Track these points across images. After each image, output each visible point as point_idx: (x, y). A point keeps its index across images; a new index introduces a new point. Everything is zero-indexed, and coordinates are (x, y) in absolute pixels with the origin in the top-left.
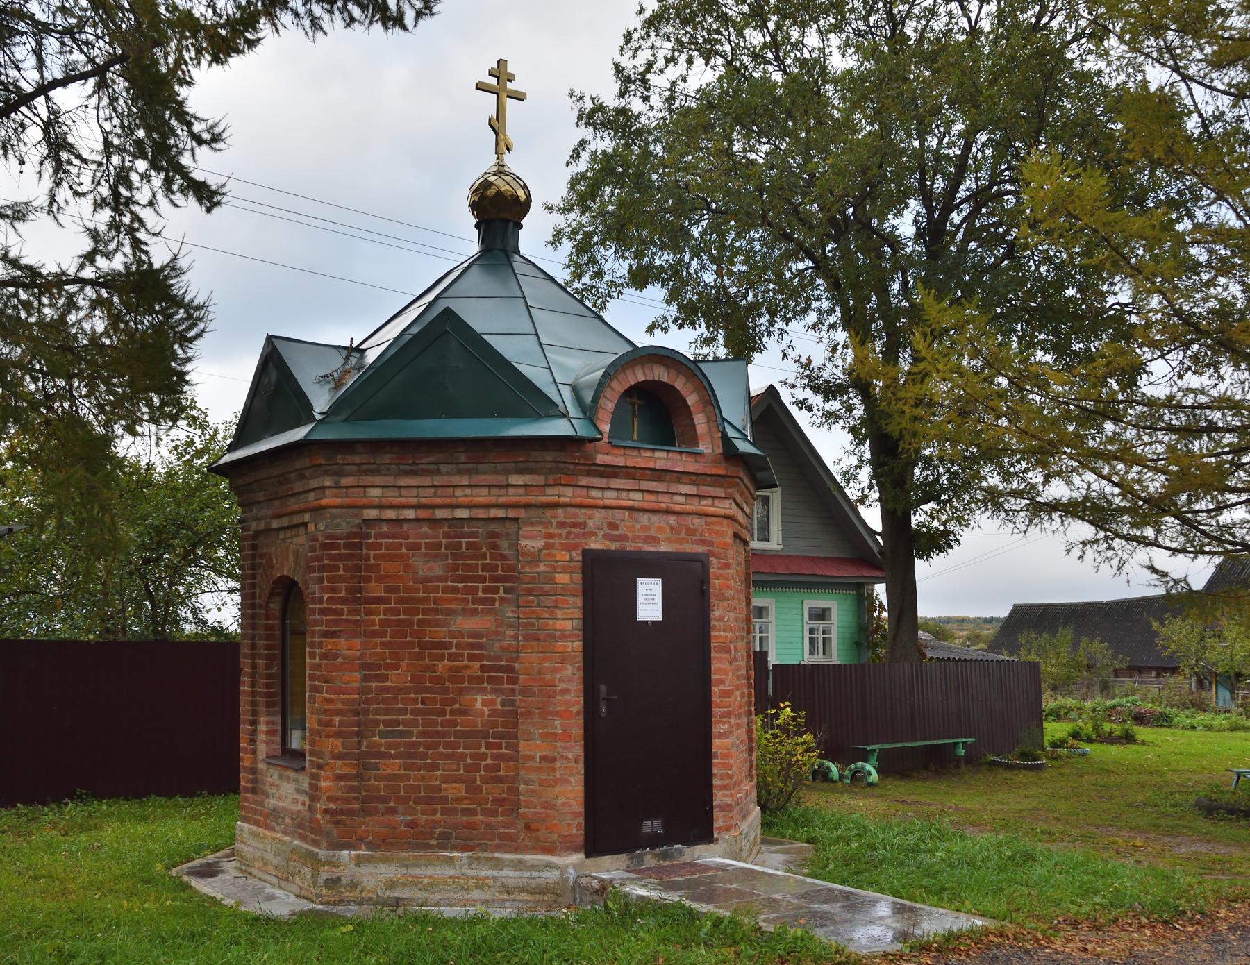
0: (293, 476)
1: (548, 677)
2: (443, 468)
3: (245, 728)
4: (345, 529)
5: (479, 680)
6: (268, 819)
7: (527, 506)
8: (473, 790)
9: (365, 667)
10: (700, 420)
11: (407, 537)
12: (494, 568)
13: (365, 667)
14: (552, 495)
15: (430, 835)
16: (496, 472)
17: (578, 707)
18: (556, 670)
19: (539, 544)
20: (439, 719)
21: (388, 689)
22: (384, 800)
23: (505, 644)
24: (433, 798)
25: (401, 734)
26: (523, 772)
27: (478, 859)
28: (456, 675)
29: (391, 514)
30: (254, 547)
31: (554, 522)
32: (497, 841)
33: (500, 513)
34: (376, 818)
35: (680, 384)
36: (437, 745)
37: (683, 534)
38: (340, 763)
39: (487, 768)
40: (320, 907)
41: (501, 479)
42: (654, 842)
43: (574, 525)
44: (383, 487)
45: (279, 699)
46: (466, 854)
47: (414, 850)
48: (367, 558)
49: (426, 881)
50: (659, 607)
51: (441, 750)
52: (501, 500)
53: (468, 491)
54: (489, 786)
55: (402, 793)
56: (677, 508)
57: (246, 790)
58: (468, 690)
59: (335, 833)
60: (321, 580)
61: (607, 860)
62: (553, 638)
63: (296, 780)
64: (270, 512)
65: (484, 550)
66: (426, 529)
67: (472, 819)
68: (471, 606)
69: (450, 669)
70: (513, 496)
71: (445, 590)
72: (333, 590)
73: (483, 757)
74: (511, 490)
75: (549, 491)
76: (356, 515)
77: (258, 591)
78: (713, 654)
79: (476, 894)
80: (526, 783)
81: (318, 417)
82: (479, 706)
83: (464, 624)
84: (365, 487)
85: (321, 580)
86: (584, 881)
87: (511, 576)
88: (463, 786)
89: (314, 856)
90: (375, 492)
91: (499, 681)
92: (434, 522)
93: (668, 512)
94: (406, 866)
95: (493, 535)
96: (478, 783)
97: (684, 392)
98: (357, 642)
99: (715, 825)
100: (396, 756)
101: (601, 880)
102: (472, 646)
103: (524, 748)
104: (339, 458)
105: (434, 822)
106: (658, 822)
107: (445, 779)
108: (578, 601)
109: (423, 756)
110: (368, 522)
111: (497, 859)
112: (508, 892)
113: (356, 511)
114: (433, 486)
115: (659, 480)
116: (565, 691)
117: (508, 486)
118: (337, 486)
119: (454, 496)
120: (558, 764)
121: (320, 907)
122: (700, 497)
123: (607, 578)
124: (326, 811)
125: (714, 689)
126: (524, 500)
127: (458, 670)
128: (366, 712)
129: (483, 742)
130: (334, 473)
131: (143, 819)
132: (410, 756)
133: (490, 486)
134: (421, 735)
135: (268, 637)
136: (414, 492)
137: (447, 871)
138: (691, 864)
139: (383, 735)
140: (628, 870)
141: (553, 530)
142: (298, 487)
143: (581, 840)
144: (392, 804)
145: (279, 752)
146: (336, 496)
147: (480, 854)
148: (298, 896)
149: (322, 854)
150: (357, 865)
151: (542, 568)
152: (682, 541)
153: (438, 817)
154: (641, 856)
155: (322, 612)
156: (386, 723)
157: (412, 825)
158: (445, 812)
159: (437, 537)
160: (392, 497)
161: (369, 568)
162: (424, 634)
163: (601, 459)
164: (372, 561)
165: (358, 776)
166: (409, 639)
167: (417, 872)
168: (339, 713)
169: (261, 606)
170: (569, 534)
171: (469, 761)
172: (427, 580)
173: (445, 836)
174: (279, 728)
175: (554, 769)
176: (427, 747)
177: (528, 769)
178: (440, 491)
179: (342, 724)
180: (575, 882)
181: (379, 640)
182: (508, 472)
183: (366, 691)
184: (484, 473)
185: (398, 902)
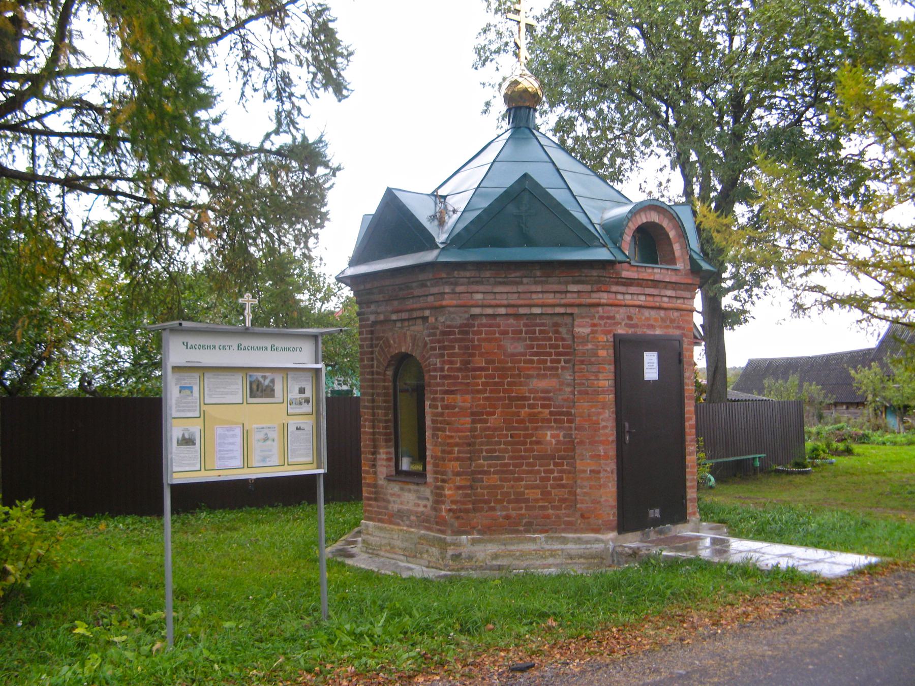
0: (414, 284)
1: (594, 418)
2: (525, 280)
3: (366, 458)
4: (458, 321)
5: (549, 421)
6: (395, 518)
7: (579, 305)
8: (546, 494)
9: (473, 414)
10: (677, 247)
11: (499, 327)
12: (557, 347)
13: (473, 414)
14: (595, 298)
15: (518, 524)
16: (559, 283)
17: (613, 438)
18: (599, 414)
19: (587, 330)
20: (523, 448)
21: (488, 428)
22: (487, 502)
23: (566, 396)
24: (519, 499)
25: (498, 458)
26: (579, 481)
27: (552, 538)
28: (533, 418)
29: (490, 311)
30: (372, 332)
31: (597, 316)
32: (563, 526)
33: (562, 310)
34: (482, 513)
35: (665, 224)
36: (522, 465)
37: (668, 323)
38: (458, 478)
39: (555, 479)
40: (449, 573)
41: (562, 288)
42: (655, 523)
43: (609, 318)
44: (484, 293)
45: (393, 437)
46: (543, 535)
47: (509, 533)
48: (473, 341)
49: (518, 553)
50: (656, 370)
51: (524, 467)
52: (563, 301)
53: (540, 296)
54: (556, 490)
55: (499, 497)
56: (665, 305)
57: (369, 499)
58: (541, 428)
59: (456, 524)
60: (442, 356)
61: (630, 536)
62: (597, 392)
63: (418, 491)
64: (389, 308)
65: (551, 334)
66: (511, 321)
67: (546, 513)
68: (542, 372)
69: (530, 414)
70: (570, 298)
71: (525, 362)
72: (451, 362)
73: (552, 472)
74: (569, 295)
75: (594, 295)
76: (465, 312)
77: (375, 363)
78: (686, 401)
79: (551, 561)
80: (581, 488)
81: (441, 246)
82: (548, 438)
83: (542, 384)
84: (472, 293)
85: (442, 356)
86: (619, 549)
87: (569, 352)
88: (539, 491)
89: (444, 541)
90: (479, 296)
91: (561, 421)
92: (517, 316)
93: (660, 308)
94: (505, 545)
95: (556, 325)
96: (549, 488)
97: (668, 229)
98: (468, 397)
99: (688, 512)
100: (495, 473)
101: (630, 548)
102: (544, 399)
103: (579, 466)
104: (456, 274)
105: (522, 515)
106: (657, 511)
107: (527, 487)
108: (612, 367)
109: (513, 472)
110: (474, 317)
111: (565, 538)
112: (571, 558)
113: (465, 309)
114: (519, 292)
115: (655, 287)
116: (605, 427)
117: (567, 292)
118: (454, 293)
119: (531, 299)
120: (602, 475)
121: (449, 573)
122: (677, 298)
123: (627, 351)
124: (450, 510)
125: (687, 424)
126: (578, 301)
127: (534, 415)
128: (474, 444)
129: (552, 462)
130: (452, 284)
131: (258, 521)
132: (503, 472)
133: (554, 292)
134: (511, 458)
135: (386, 395)
136: (505, 296)
137: (531, 547)
138: (676, 537)
139: (485, 459)
140: (641, 541)
141: (596, 321)
142: (417, 292)
143: (615, 523)
144: (492, 504)
145: (394, 473)
146: (452, 299)
147: (552, 535)
148: (427, 567)
149: (449, 538)
150: (472, 544)
151: (590, 346)
152: (667, 327)
153: (523, 511)
154: (648, 532)
155: (443, 377)
156: (487, 451)
157: (508, 517)
158: (527, 508)
159: (519, 326)
160: (490, 299)
161: (474, 347)
162: (512, 391)
163: (625, 274)
164: (476, 343)
165: (471, 487)
166: (501, 394)
167: (513, 548)
168: (457, 445)
169: (378, 373)
170: (605, 323)
171: (543, 474)
172: (513, 355)
173: (529, 524)
174: (393, 456)
175: (599, 478)
176: (515, 465)
177: (582, 478)
178: (522, 296)
179: (459, 452)
180: (613, 550)
181: (482, 396)
182: (567, 283)
183: (475, 430)
184: (553, 283)
185: (500, 568)
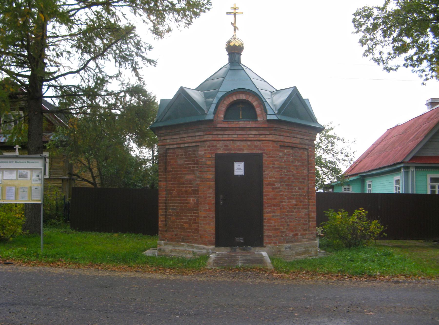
2: (181, 132)
5: (191, 194)
7: (200, 142)
8: (190, 226)
17: (213, 202)
25: (175, 209)
29: (171, 147)
35: (250, 99)
37: (253, 147)
41: (193, 134)
42: (240, 245)
43: (213, 146)
49: (178, 251)
53: (187, 138)
61: (223, 249)
66: (180, 150)
70: (197, 139)
74: (197, 137)
75: (206, 136)
82: (191, 201)
90: (168, 141)
94: (174, 246)
99: (264, 242)
100: (175, 216)
103: (200, 215)
116: (209, 197)
117: (196, 136)
120: (207, 219)
123: (224, 163)
133: (192, 137)
141: (206, 148)
143: (214, 242)
151: (204, 160)
170: (211, 149)
173: (183, 239)
175: (206, 220)
